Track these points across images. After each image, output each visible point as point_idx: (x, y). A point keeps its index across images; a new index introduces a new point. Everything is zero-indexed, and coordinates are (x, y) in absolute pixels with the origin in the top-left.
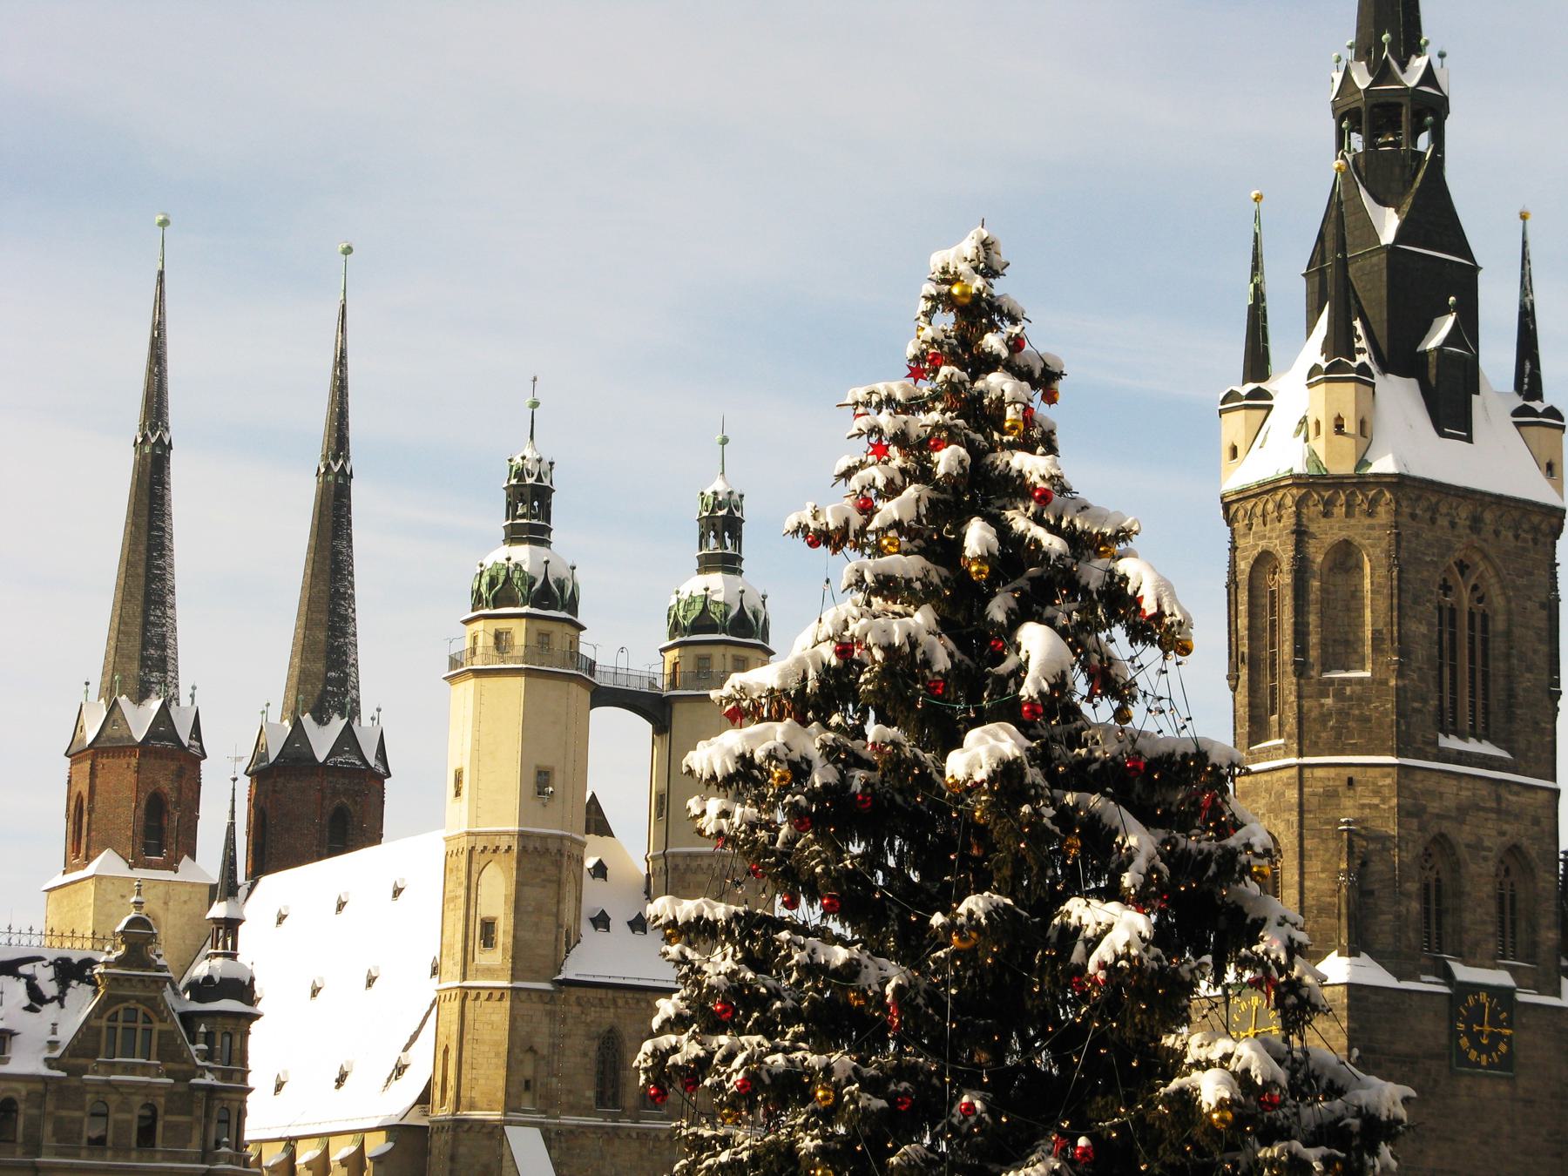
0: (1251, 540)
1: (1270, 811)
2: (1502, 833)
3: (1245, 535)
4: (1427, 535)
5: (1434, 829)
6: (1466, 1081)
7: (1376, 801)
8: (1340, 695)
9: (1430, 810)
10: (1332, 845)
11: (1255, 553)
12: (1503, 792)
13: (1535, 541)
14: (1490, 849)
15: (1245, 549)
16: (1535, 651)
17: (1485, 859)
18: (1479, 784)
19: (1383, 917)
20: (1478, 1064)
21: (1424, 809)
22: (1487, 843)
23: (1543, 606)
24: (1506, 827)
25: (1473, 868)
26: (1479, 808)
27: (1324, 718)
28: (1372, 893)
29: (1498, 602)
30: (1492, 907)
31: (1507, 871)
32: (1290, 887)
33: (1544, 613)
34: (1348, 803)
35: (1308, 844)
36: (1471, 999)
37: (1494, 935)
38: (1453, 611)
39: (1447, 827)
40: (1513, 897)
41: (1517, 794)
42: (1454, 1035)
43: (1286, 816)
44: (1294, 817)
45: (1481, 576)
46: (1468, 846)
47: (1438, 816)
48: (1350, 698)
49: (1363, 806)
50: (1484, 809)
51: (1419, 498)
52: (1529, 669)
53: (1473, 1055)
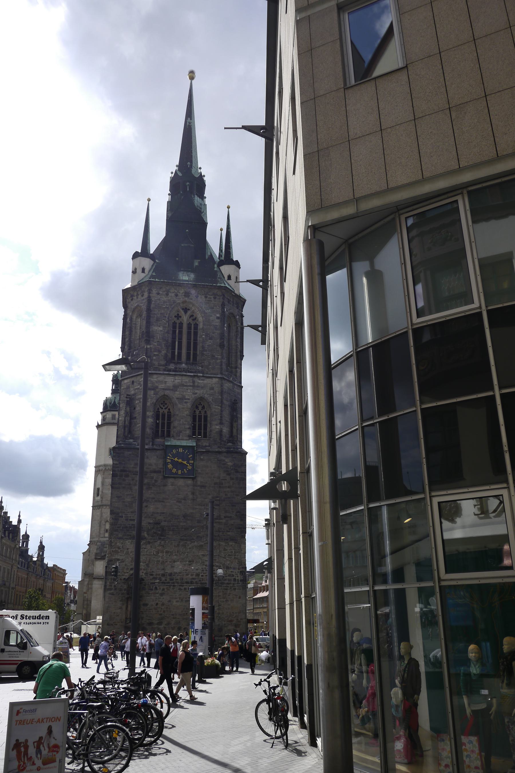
2: (196, 394)
4: (164, 298)
5: (161, 393)
6: (170, 481)
7: (139, 387)
9: (159, 387)
12: (196, 379)
13: (215, 298)
14: (189, 399)
16: (214, 333)
17: (186, 403)
18: (184, 378)
19: (138, 425)
20: (176, 474)
21: (157, 387)
22: (187, 397)
23: (218, 318)
24: (196, 391)
25: (180, 406)
26: (184, 386)
28: (135, 418)
29: (200, 319)
30: (190, 419)
31: (203, 407)
33: (218, 320)
36: (174, 451)
37: (189, 428)
38: (181, 324)
39: (167, 392)
40: (206, 417)
41: (203, 380)
42: (166, 464)
45: (193, 312)
46: (177, 398)
47: (163, 389)
50: (186, 386)
51: (161, 288)
52: (211, 339)
53: (174, 470)
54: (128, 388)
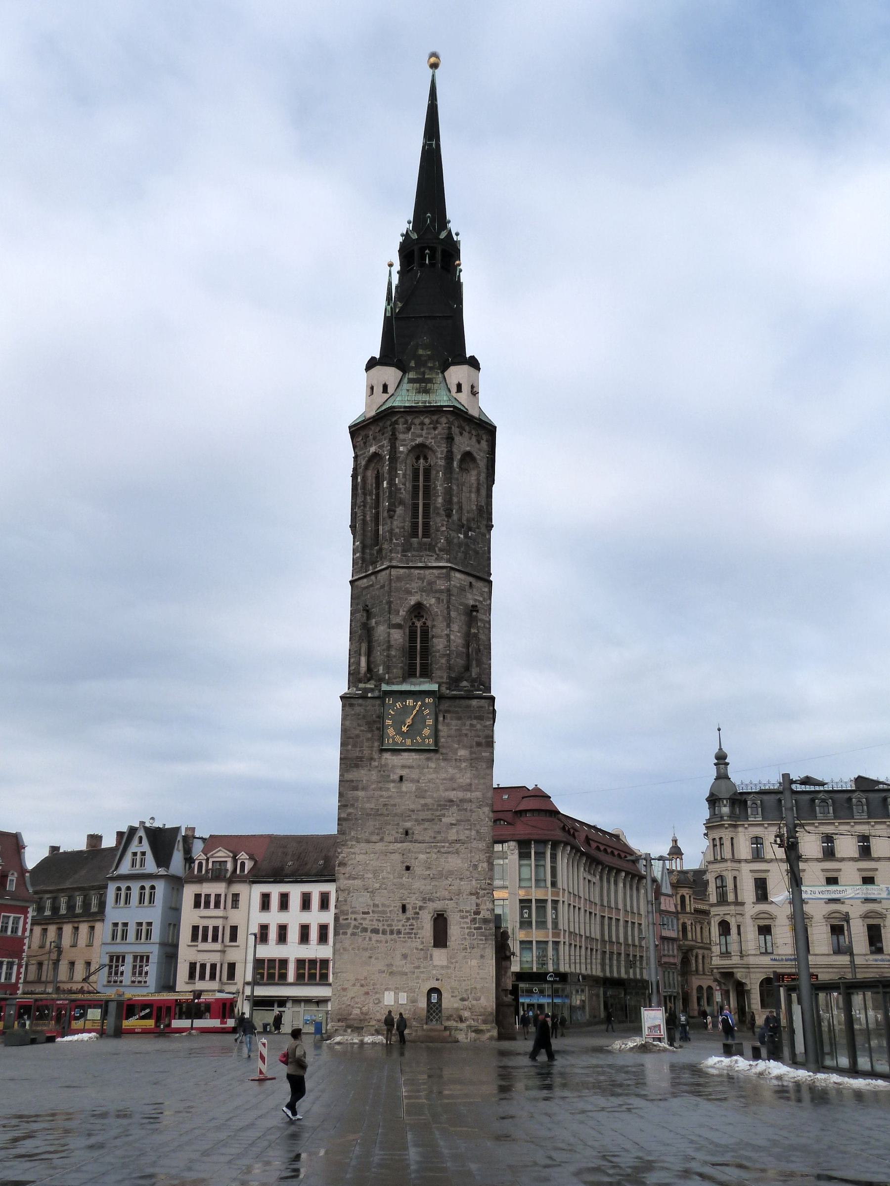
0: (410, 436)
1: (422, 590)
3: (404, 433)
7: (481, 599)
8: (466, 536)
10: (463, 618)
11: (413, 444)
15: (404, 440)
27: (460, 545)
32: (440, 637)
34: (469, 596)
35: (453, 614)
43: (437, 595)
44: (444, 597)
48: (469, 538)
49: (476, 600)
54: (462, 589)
